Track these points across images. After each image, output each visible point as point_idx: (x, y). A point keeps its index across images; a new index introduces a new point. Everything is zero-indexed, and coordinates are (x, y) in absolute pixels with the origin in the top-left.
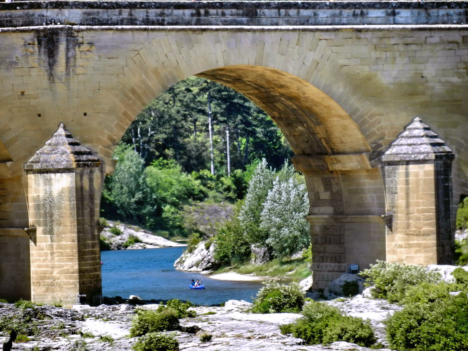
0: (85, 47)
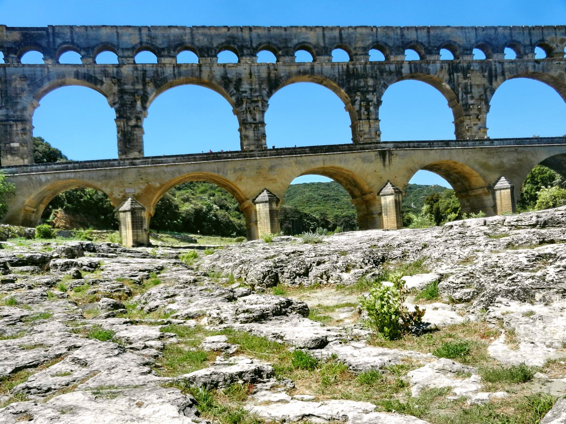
0: (394, 156)
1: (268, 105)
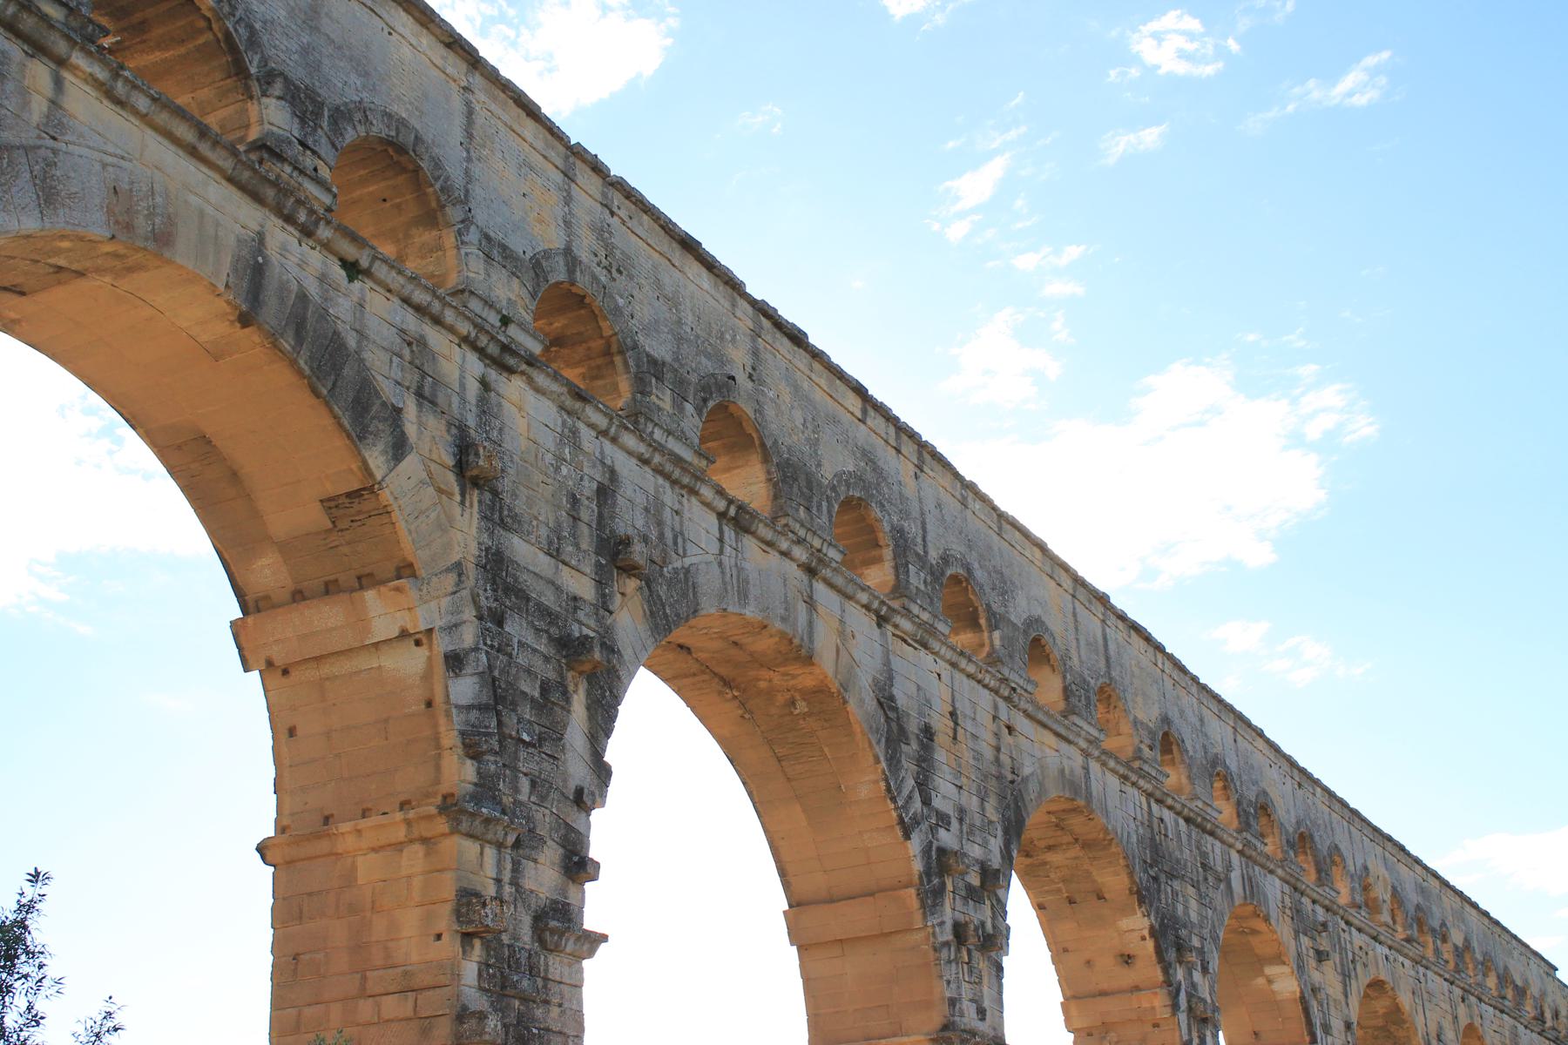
1: (1008, 928)
